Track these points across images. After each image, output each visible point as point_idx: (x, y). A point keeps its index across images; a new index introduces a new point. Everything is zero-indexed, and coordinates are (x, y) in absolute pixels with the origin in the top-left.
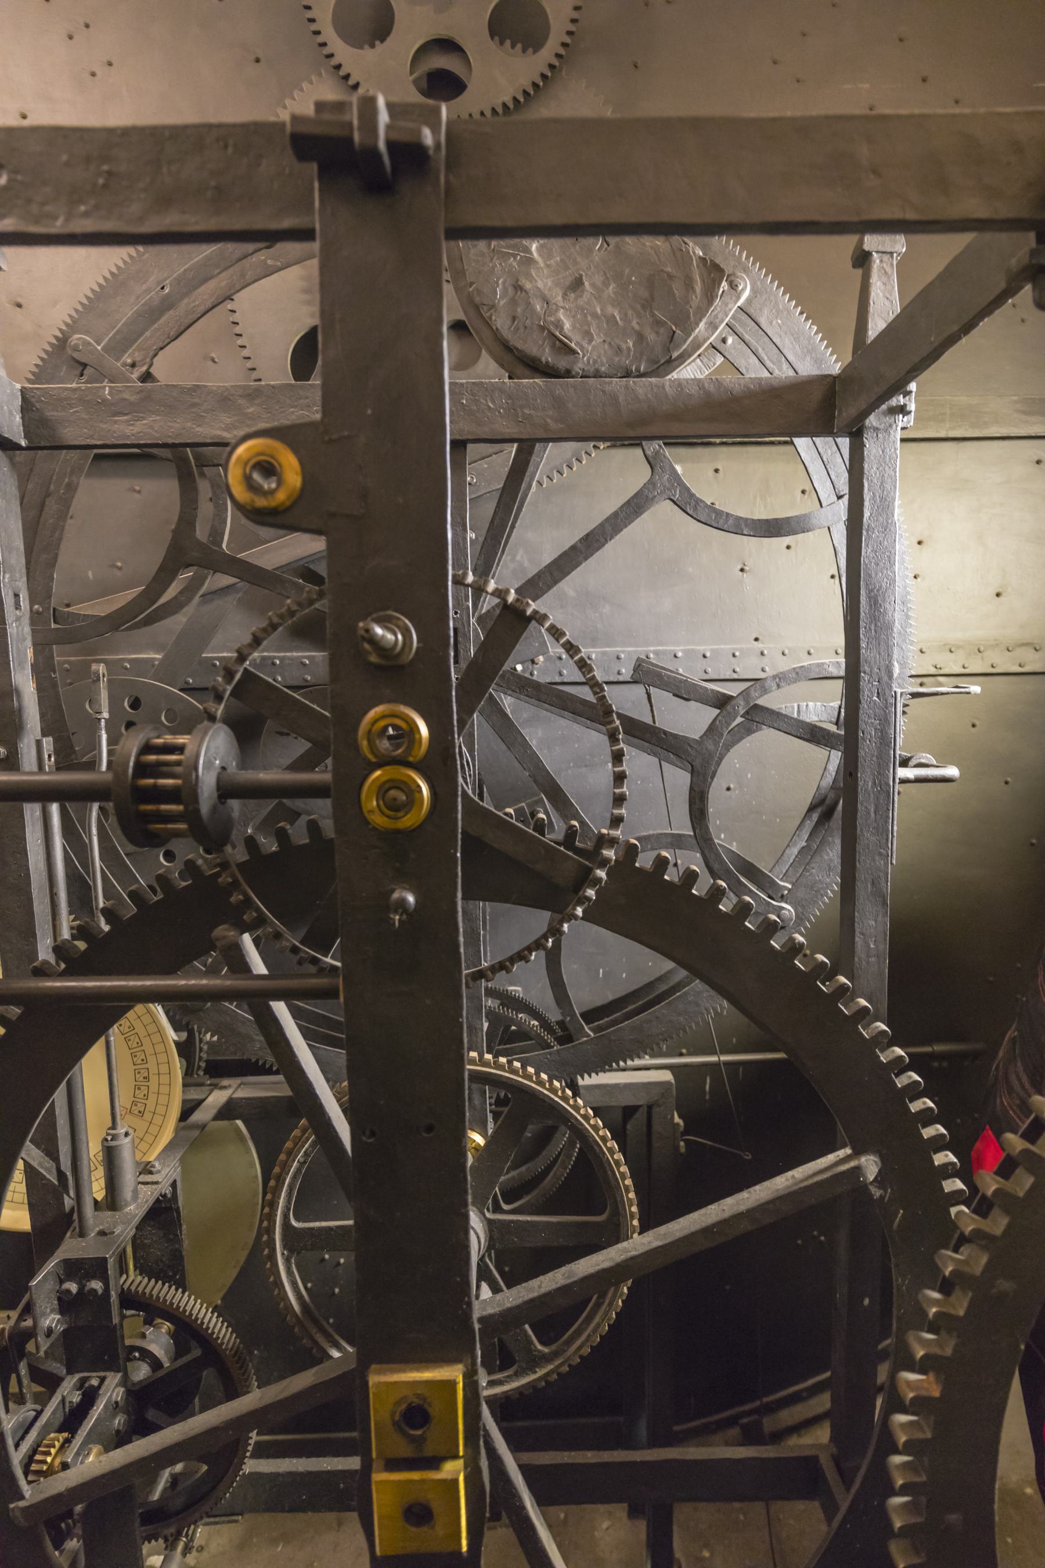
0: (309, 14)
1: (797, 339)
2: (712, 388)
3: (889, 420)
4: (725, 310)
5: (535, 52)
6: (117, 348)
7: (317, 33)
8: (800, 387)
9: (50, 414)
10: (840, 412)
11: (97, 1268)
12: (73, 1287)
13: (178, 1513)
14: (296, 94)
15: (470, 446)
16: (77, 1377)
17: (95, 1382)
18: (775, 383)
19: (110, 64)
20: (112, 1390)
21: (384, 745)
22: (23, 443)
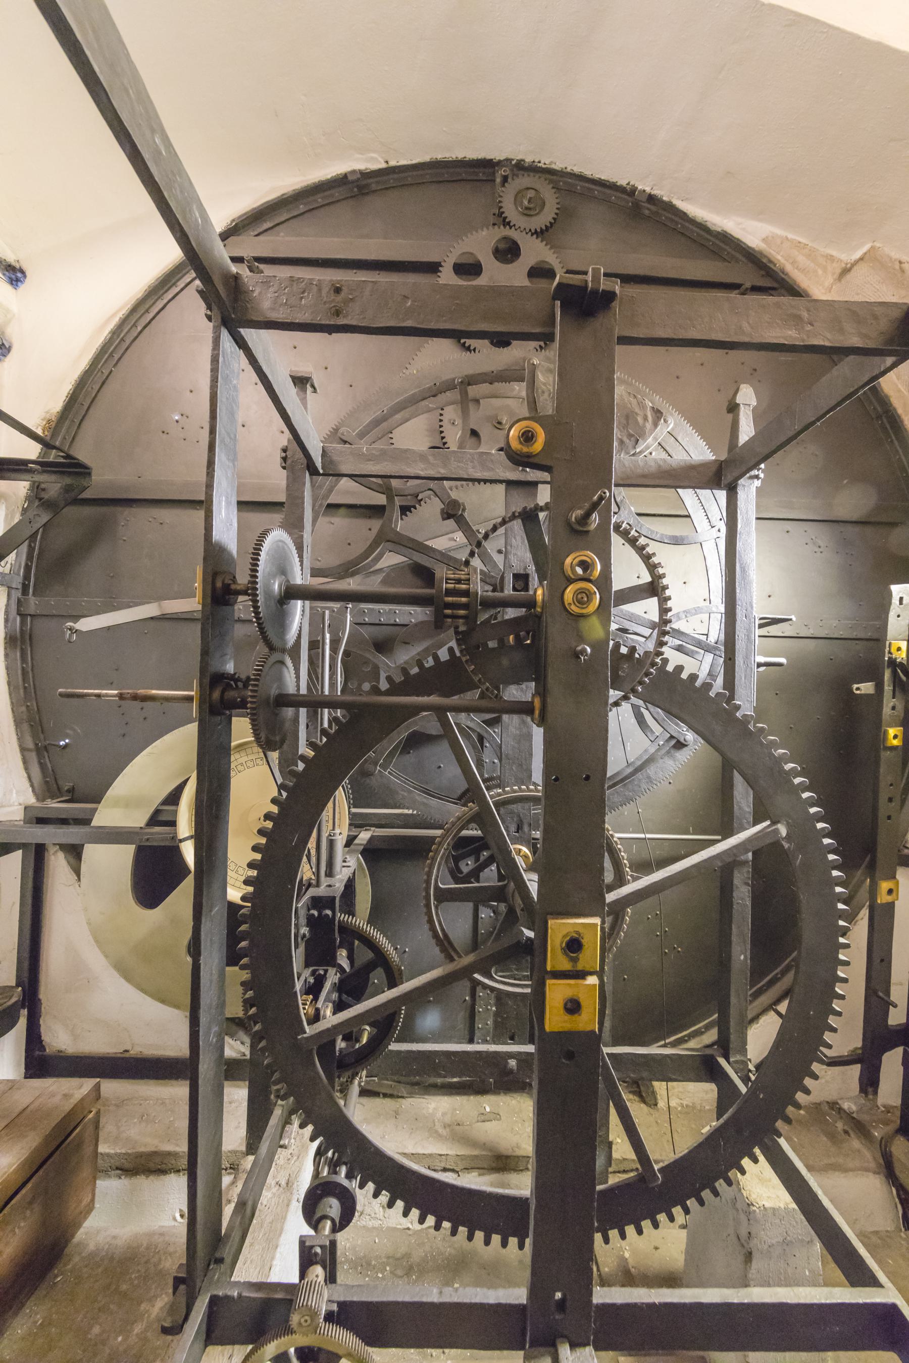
1: (696, 448)
2: (661, 463)
3: (750, 481)
4: (662, 431)
6: (362, 435)
8: (705, 465)
9: (335, 458)
10: (726, 476)
11: (329, 902)
12: (316, 913)
13: (353, 1064)
15: (540, 486)
16: (311, 969)
17: (322, 972)
18: (693, 463)
20: (332, 978)
21: (579, 571)
22: (321, 472)
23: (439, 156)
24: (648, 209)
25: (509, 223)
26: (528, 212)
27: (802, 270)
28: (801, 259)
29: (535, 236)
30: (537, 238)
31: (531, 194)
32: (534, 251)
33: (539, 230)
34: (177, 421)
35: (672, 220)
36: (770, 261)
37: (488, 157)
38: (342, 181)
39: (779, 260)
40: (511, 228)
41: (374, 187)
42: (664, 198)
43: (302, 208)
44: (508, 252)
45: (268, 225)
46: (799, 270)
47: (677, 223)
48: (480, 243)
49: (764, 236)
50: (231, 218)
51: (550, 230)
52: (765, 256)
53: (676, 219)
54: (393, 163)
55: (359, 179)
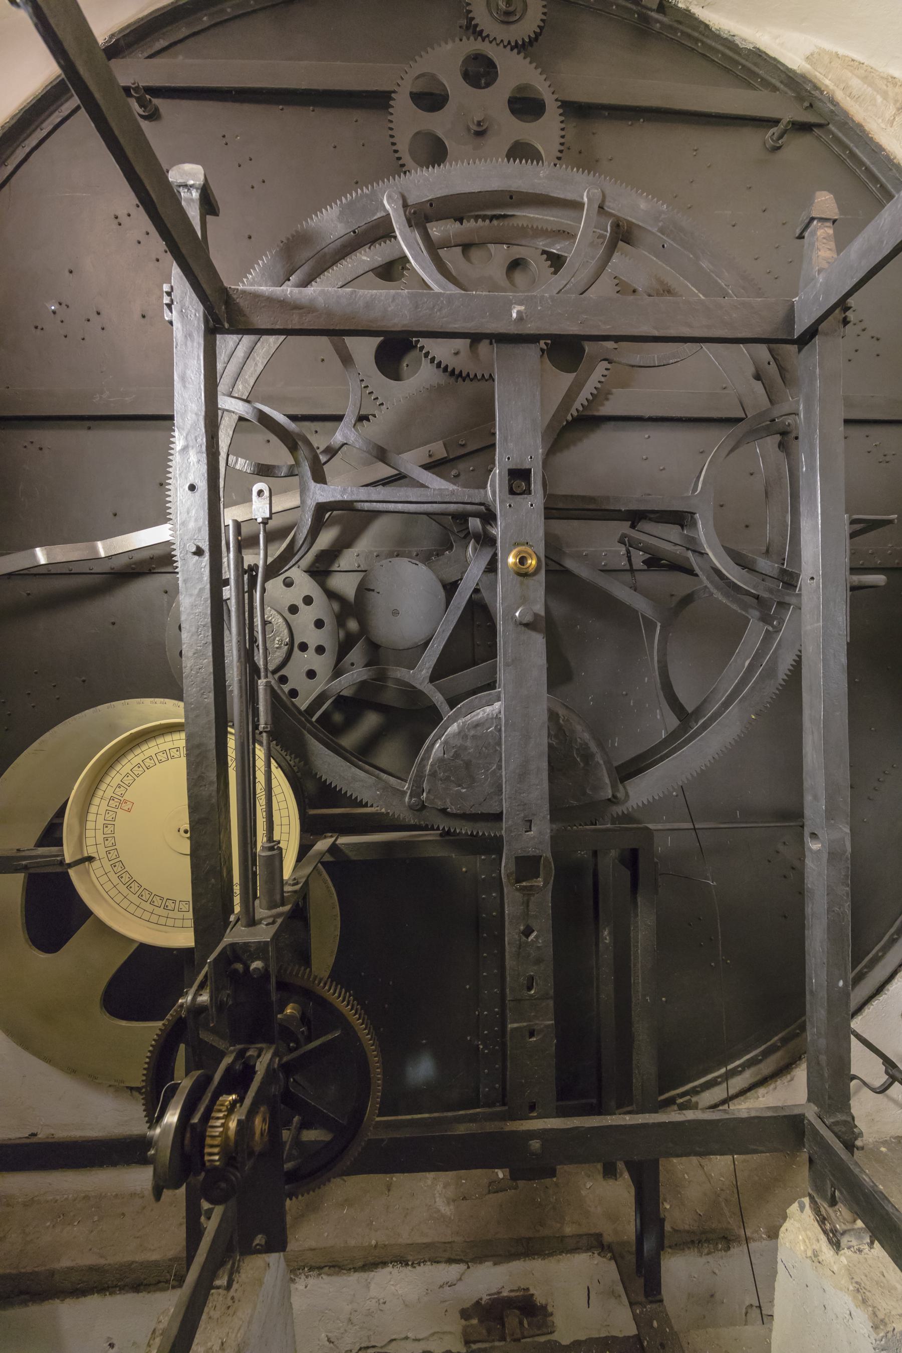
7: (399, 159)
19: (264, 182)
24: (657, 21)
26: (508, 17)
27: (856, 99)
28: (856, 83)
29: (516, 51)
30: (519, 53)
32: (515, 71)
33: (520, 43)
34: (54, 312)
35: (689, 36)
36: (816, 87)
39: (827, 86)
40: (483, 40)
42: (680, 5)
44: (480, 72)
45: (162, 43)
46: (852, 98)
47: (697, 40)
48: (445, 60)
49: (808, 53)
50: (110, 33)
52: (810, 81)
53: (696, 34)
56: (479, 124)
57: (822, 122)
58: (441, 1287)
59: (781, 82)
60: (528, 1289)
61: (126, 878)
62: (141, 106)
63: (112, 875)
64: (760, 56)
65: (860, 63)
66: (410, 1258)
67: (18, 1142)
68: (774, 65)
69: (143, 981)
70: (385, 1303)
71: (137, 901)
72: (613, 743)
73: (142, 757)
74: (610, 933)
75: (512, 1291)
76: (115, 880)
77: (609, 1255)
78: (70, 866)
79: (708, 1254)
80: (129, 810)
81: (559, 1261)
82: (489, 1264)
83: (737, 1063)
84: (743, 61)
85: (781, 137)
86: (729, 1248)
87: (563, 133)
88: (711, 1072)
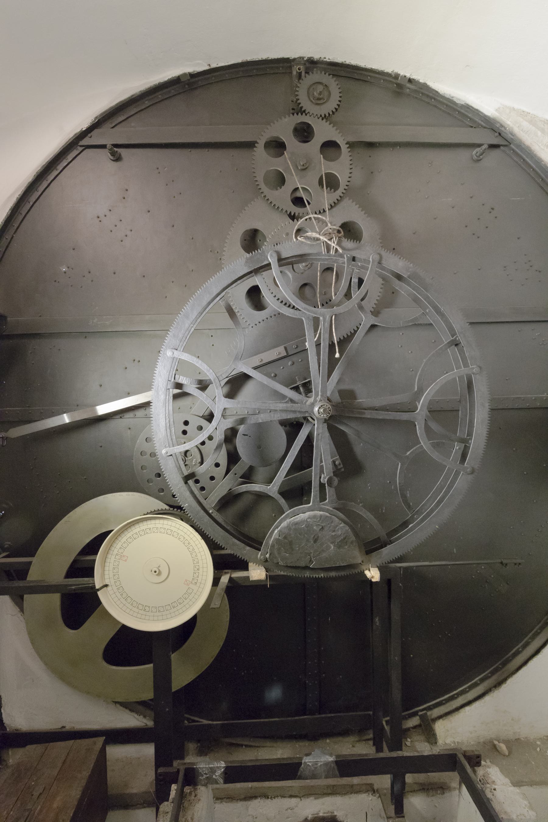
0: (255, 179)
5: (334, 192)
14: (249, 205)
23: (249, 59)
24: (409, 89)
25: (304, 111)
26: (319, 101)
28: (525, 124)
29: (325, 120)
31: (320, 88)
33: (327, 115)
34: (65, 273)
36: (502, 126)
37: (286, 56)
38: (175, 82)
39: (508, 125)
40: (306, 115)
41: (200, 83)
42: (421, 81)
43: (147, 103)
47: (431, 98)
48: (283, 128)
50: (95, 116)
51: (336, 113)
52: (498, 122)
53: (431, 95)
54: (214, 66)
55: (189, 80)
56: (303, 165)
57: (506, 143)
58: (286, 810)
59: (482, 121)
60: (333, 812)
61: (124, 595)
62: (112, 156)
63: (117, 594)
64: (468, 108)
65: (528, 113)
66: (269, 794)
67: (55, 731)
68: (477, 112)
69: (128, 647)
70: (256, 818)
71: (131, 607)
72: (382, 510)
73: (132, 533)
74: (379, 620)
75: (324, 813)
76: (119, 596)
77: (378, 795)
78: (98, 590)
79: (432, 796)
80: (126, 561)
81: (350, 798)
82: (312, 798)
83: (455, 692)
84: (459, 109)
85: (481, 154)
86: (444, 793)
87: (351, 167)
88: (439, 698)
